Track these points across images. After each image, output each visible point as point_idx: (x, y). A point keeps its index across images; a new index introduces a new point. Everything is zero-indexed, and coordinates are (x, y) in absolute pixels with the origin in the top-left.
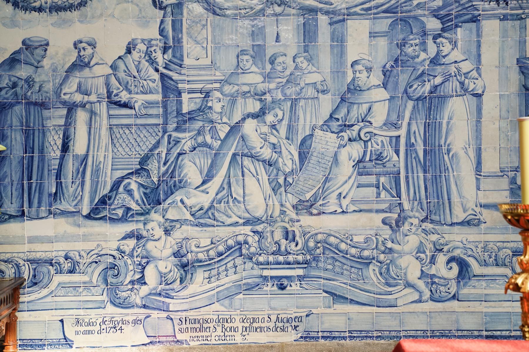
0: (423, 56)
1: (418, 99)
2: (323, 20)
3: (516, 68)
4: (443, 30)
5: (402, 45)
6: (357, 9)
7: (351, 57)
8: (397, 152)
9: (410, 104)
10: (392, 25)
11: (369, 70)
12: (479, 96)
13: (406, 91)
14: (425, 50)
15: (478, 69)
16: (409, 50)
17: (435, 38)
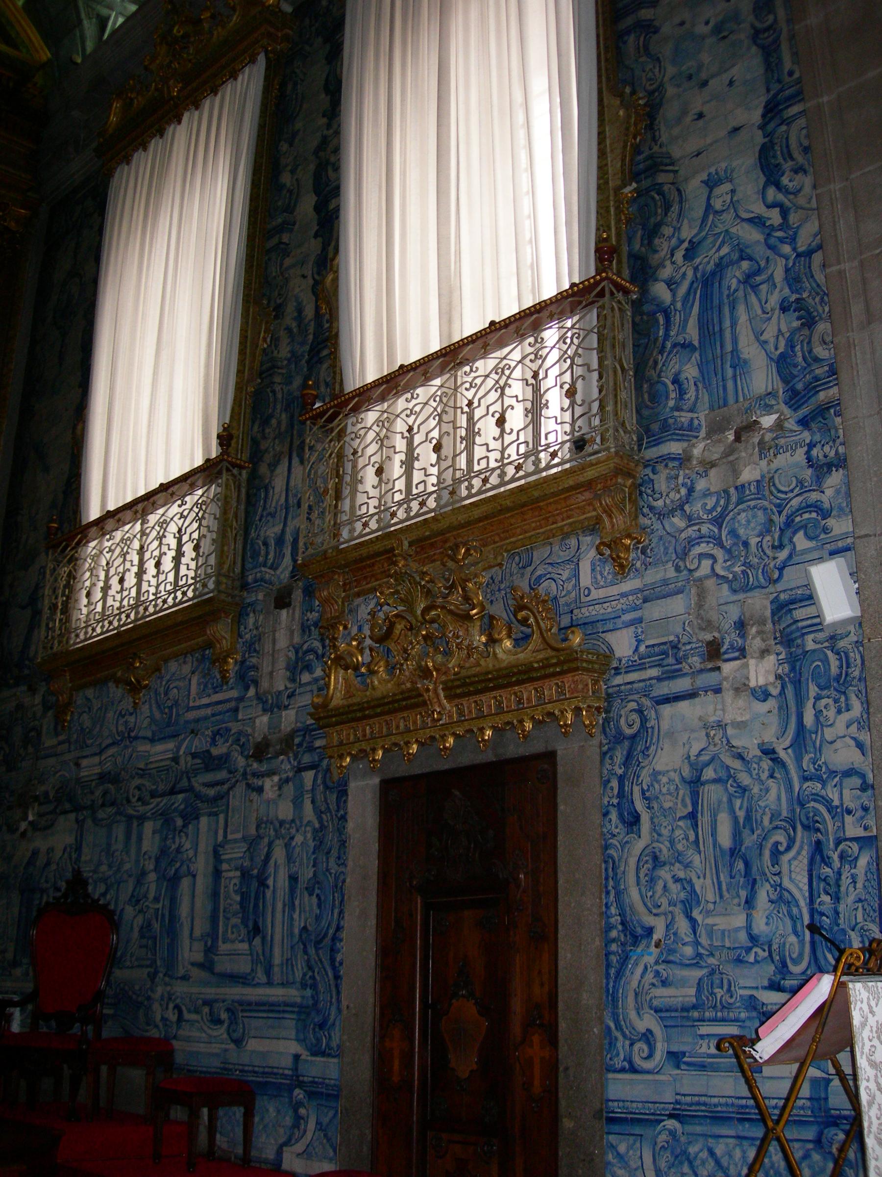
0: (173, 847)
1: (169, 880)
2: (135, 824)
3: (212, 853)
4: (184, 826)
5: (166, 839)
6: (149, 814)
7: (144, 849)
8: (157, 921)
9: (165, 884)
10: (162, 825)
11: (150, 858)
12: (194, 876)
13: (164, 875)
14: (174, 842)
15: (196, 855)
16: (168, 842)
17: (181, 831)
